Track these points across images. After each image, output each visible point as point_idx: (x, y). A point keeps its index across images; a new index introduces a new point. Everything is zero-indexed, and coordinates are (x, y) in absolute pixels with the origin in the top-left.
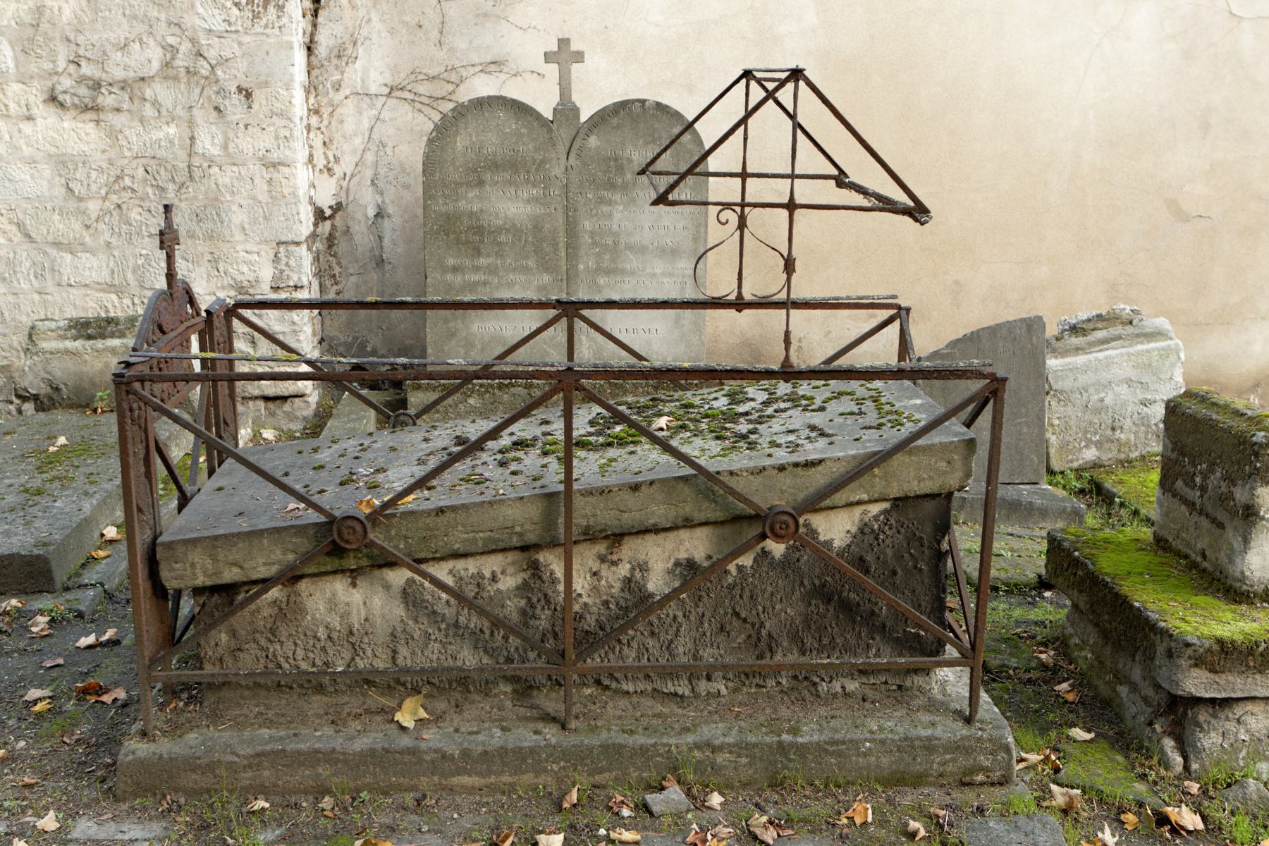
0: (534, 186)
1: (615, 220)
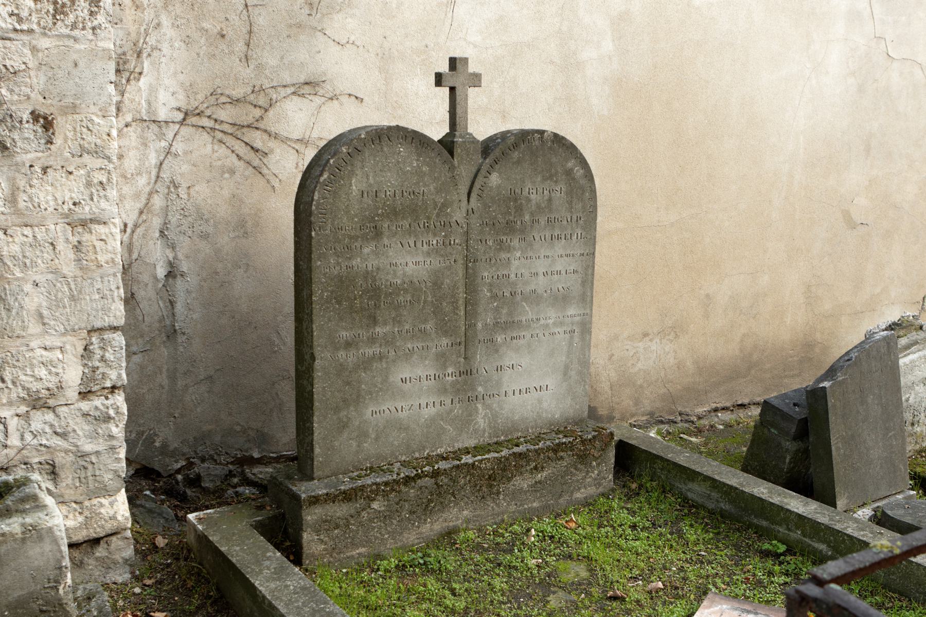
0: (435, 235)
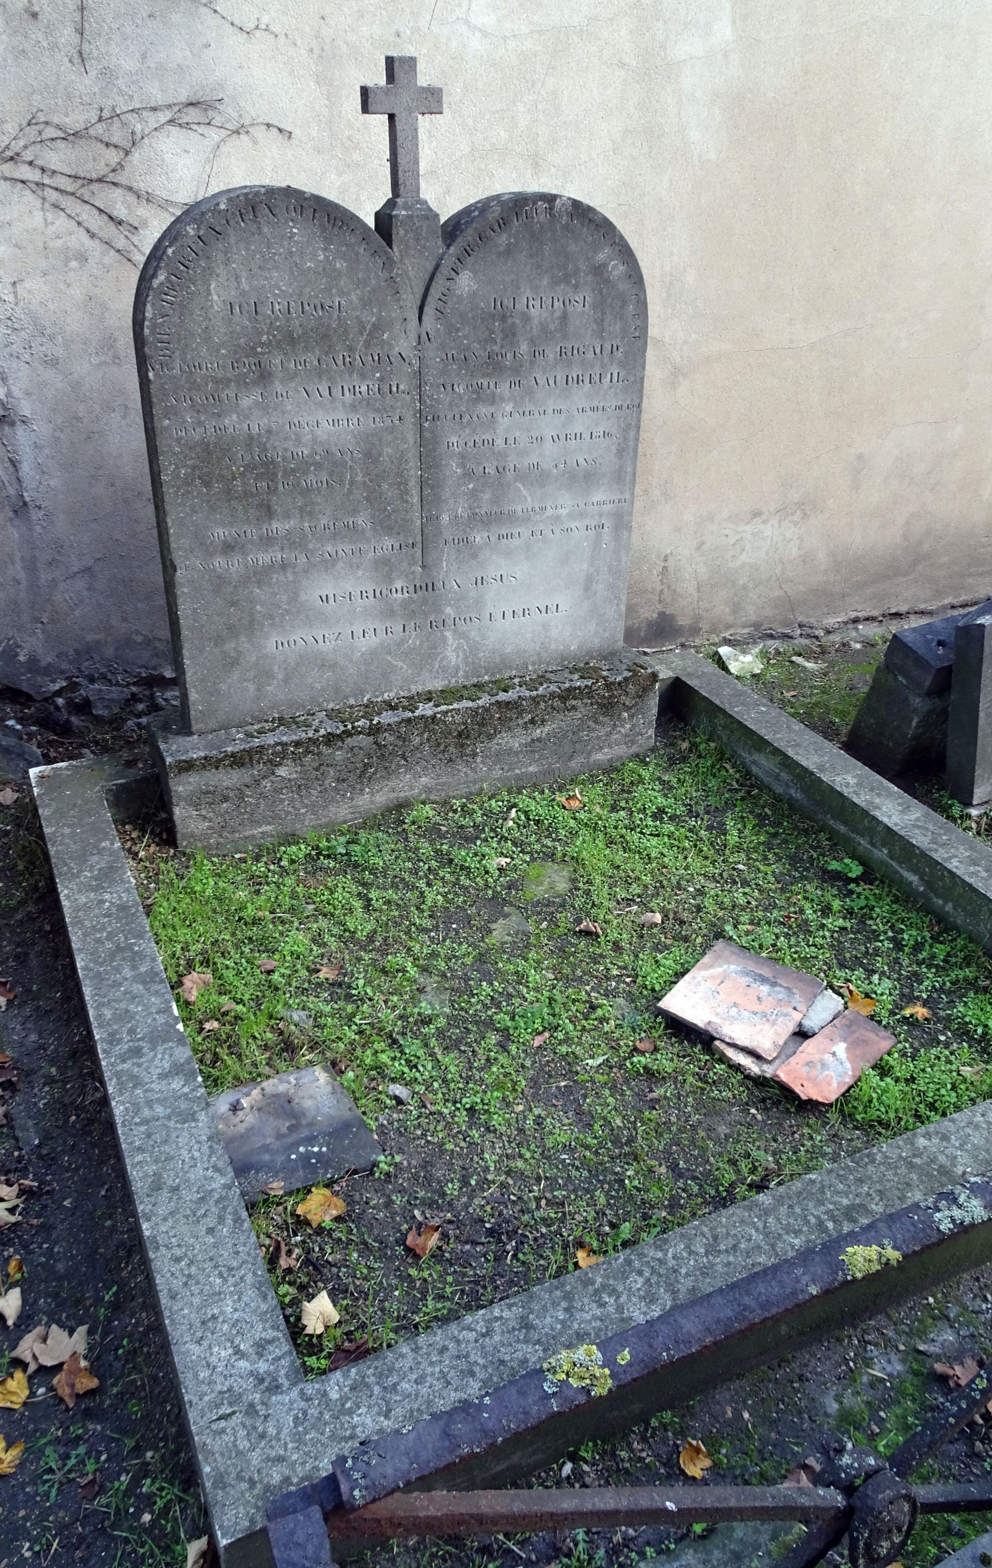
0: (363, 377)
1: (500, 430)
